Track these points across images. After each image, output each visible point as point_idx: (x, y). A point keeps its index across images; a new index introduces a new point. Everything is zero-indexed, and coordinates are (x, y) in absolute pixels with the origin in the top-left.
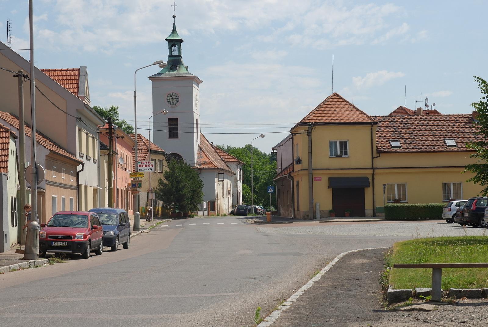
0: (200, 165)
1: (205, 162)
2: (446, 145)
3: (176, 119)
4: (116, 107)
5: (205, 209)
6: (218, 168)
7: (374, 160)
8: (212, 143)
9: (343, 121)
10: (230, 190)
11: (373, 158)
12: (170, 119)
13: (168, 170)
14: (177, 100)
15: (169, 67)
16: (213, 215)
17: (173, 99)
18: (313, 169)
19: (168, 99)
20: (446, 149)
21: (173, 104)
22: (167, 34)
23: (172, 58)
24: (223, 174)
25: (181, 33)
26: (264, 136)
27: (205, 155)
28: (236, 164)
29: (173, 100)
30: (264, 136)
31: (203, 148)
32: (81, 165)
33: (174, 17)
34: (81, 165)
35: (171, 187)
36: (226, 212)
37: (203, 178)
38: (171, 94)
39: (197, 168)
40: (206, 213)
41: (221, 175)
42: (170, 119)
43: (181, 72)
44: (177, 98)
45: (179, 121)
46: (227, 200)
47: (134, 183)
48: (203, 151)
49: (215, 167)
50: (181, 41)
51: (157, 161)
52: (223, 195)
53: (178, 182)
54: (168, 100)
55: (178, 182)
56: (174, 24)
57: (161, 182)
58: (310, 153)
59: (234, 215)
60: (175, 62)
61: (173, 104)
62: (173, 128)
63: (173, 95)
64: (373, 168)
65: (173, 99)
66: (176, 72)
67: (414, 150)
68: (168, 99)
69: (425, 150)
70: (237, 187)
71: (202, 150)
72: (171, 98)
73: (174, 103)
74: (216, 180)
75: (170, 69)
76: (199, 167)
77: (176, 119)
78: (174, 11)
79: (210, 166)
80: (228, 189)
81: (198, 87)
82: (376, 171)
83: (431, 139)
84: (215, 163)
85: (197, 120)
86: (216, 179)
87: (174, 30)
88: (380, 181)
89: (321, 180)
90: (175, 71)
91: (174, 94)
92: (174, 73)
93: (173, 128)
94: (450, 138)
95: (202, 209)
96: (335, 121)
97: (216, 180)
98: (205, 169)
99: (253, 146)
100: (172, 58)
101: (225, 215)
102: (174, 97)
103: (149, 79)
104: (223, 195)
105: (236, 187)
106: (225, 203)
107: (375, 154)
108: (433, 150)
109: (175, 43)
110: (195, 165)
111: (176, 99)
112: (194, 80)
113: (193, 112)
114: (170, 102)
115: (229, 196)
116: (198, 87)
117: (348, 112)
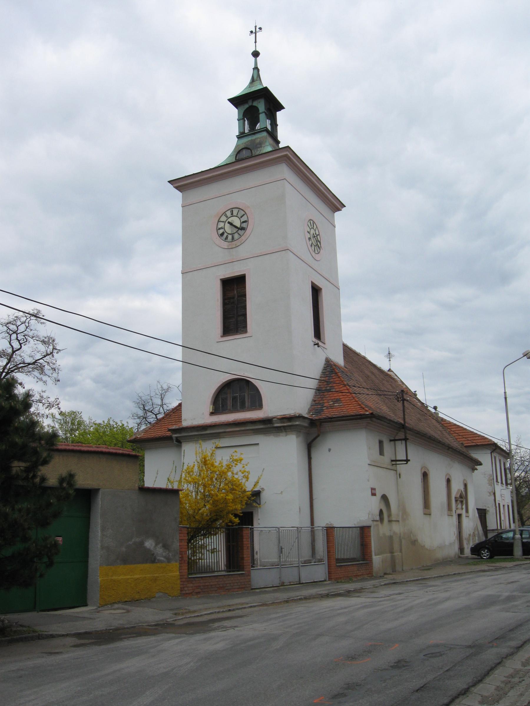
8: (435, 408)
19: (220, 229)
33: (256, 54)
38: (229, 214)
52: (427, 504)
54: (221, 231)
56: (256, 69)
63: (232, 214)
68: (220, 229)
70: (494, 494)
78: (255, 42)
91: (235, 212)
98: (331, 420)
100: (245, 140)
103: (170, 186)
104: (427, 504)
105: (492, 494)
109: (257, 106)
114: (225, 234)
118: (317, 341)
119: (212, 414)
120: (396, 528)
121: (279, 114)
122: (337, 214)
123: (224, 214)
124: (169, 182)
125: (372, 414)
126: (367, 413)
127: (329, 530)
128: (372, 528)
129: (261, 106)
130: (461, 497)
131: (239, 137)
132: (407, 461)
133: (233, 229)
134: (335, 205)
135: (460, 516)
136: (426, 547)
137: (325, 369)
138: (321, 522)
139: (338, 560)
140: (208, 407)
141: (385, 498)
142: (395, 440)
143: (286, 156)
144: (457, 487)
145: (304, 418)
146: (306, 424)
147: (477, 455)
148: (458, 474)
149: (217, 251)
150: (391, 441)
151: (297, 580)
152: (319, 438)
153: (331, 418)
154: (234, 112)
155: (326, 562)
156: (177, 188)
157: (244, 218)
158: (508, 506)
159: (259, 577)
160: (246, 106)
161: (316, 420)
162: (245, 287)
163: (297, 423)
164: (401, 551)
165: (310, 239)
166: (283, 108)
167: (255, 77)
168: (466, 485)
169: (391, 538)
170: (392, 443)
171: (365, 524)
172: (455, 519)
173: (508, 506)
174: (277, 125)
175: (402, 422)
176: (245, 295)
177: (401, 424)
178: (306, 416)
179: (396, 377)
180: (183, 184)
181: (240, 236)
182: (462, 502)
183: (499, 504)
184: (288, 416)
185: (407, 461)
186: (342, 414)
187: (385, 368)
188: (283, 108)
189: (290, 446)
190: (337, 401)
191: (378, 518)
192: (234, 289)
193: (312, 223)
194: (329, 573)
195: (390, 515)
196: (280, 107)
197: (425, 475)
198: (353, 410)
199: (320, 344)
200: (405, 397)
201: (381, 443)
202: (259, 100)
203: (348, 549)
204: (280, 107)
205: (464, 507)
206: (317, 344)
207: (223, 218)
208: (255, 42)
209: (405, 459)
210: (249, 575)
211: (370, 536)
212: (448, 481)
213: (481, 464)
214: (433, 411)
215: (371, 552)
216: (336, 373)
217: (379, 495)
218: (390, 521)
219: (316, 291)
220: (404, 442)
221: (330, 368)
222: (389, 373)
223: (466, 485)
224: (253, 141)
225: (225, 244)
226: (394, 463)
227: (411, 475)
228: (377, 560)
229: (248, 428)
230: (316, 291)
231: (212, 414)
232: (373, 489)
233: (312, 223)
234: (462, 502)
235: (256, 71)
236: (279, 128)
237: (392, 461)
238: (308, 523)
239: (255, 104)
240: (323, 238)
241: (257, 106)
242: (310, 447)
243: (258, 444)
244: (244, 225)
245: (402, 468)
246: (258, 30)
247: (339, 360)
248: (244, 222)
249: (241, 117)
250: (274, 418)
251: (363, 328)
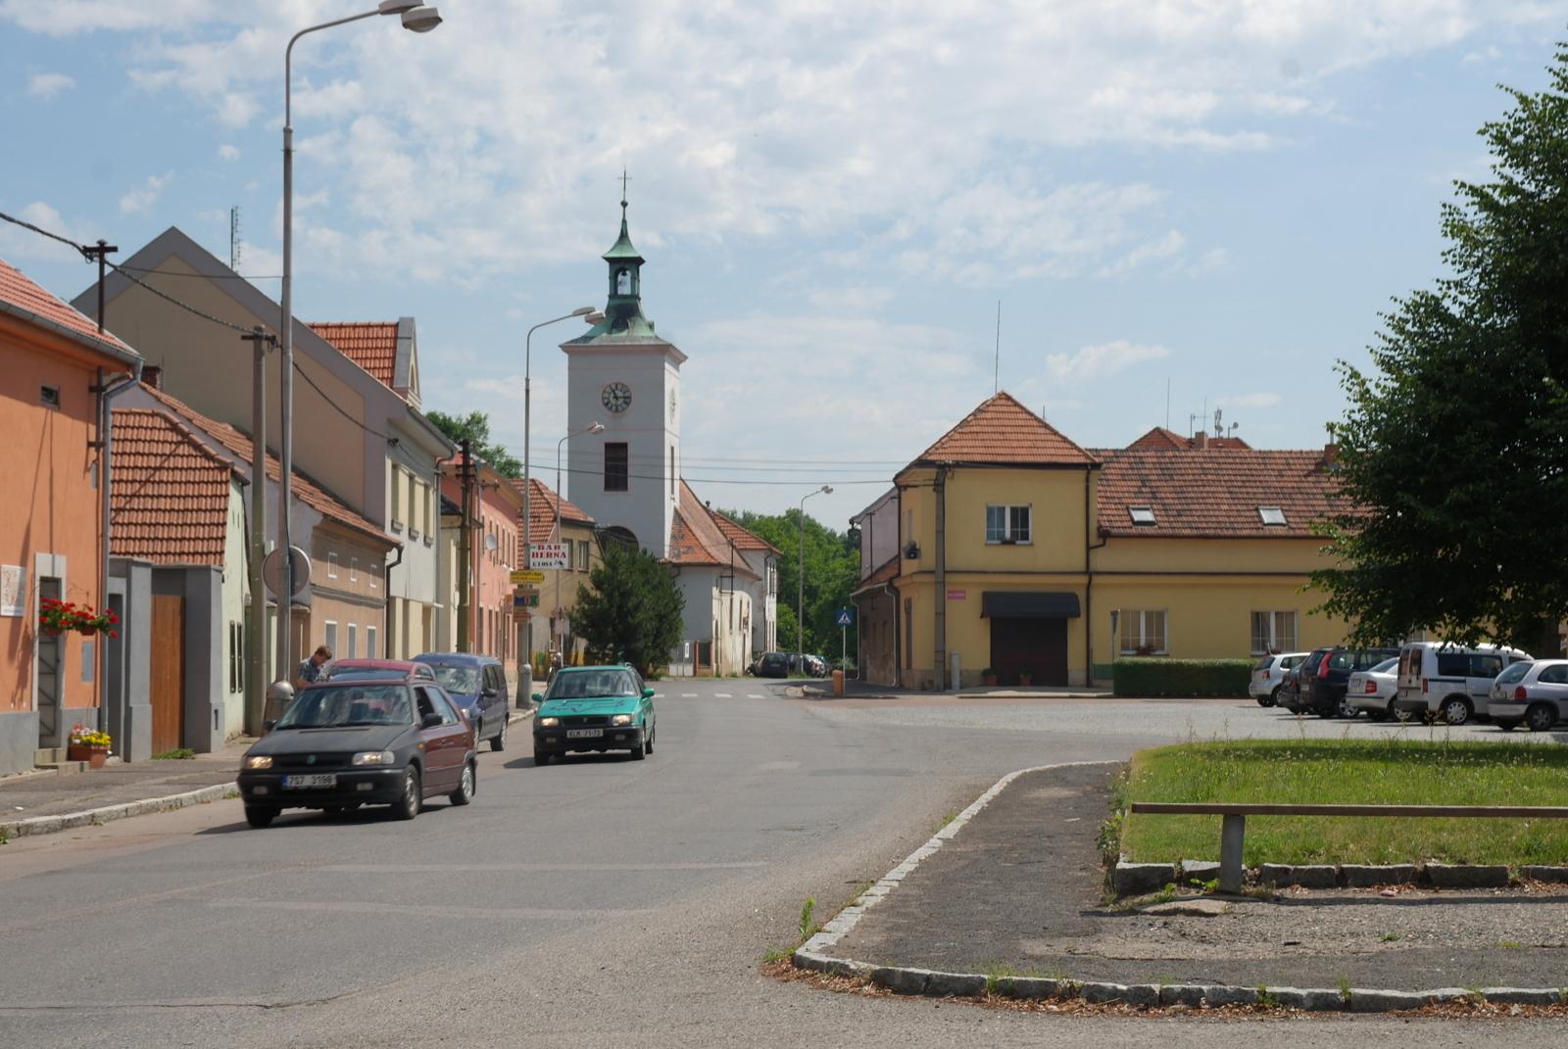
0: (678, 556)
1: (689, 548)
2: (1261, 521)
3: (624, 446)
4: (483, 416)
5: (688, 661)
6: (719, 565)
7: (1093, 553)
8: (708, 503)
9: (1019, 459)
10: (748, 617)
11: (1089, 548)
12: (609, 447)
13: (601, 566)
14: (627, 400)
15: (610, 323)
16: (705, 675)
17: (616, 397)
18: (945, 572)
20: (1261, 533)
21: (617, 408)
22: (607, 247)
23: (617, 302)
24: (732, 577)
25: (641, 242)
26: (832, 490)
27: (690, 531)
28: (763, 555)
29: (618, 400)
30: (832, 490)
31: (685, 514)
32: (395, 551)
33: (624, 204)
34: (395, 551)
35: (607, 606)
36: (738, 669)
38: (614, 387)
39: (670, 562)
40: (689, 670)
41: (727, 582)
42: (609, 447)
43: (638, 334)
44: (627, 395)
45: (631, 451)
46: (739, 639)
47: (520, 596)
48: (685, 522)
49: (713, 561)
50: (639, 261)
51: (575, 545)
52: (731, 627)
53: (626, 595)
54: (606, 401)
55: (626, 595)
56: (624, 222)
57: (584, 595)
58: (940, 532)
59: (757, 675)
60: (623, 311)
61: (617, 408)
62: (616, 466)
64: (1088, 572)
65: (616, 397)
66: (624, 334)
67: (1187, 532)
69: (1212, 532)
70: (765, 609)
71: (682, 519)
72: (612, 395)
73: (620, 409)
74: (715, 591)
75: (612, 327)
76: (674, 560)
77: (624, 446)
79: (702, 558)
80: (744, 615)
81: (678, 370)
82: (1096, 580)
83: (1226, 507)
84: (713, 551)
85: (672, 449)
86: (714, 589)
87: (624, 236)
88: (1103, 604)
89: (964, 598)
90: (622, 331)
91: (619, 387)
92: (622, 337)
93: (616, 466)
94: (1271, 506)
95: (681, 660)
96: (1000, 459)
97: (715, 591)
99: (805, 514)
101: (734, 675)
102: (619, 394)
104: (731, 627)
106: (734, 648)
107: (1094, 540)
108: (1231, 532)
109: (624, 266)
110: (667, 555)
111: (624, 397)
112: (665, 352)
113: (664, 429)
115: (745, 631)
116: (678, 370)
117: (1031, 437)
131: (610, 297)
172: (742, 636)
181: (624, 409)
186: (697, 561)
225: (610, 413)
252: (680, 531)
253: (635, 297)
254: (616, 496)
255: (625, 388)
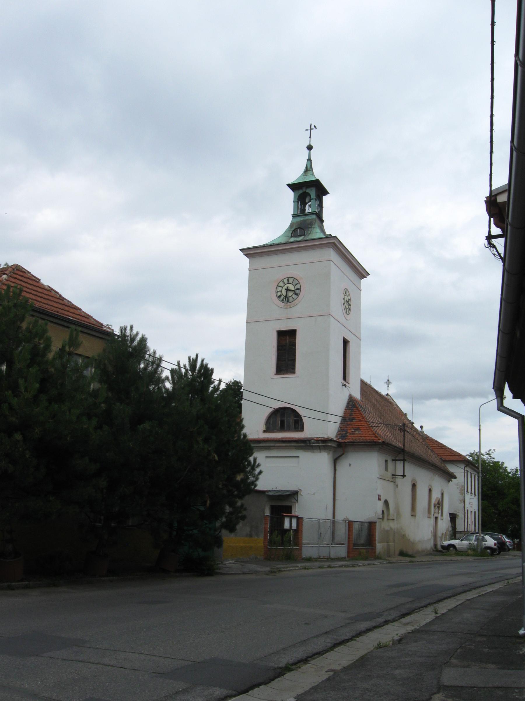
3: (292, 333)
15: (290, 235)
33: (310, 148)
37: (350, 465)
54: (279, 294)
56: (309, 160)
63: (288, 282)
70: (464, 502)
77: (292, 333)
78: (310, 137)
87: (308, 169)
99: (505, 466)
100: (298, 219)
103: (241, 253)
109: (309, 192)
114: (282, 297)
118: (344, 383)
119: (264, 431)
120: (393, 525)
121: (325, 198)
122: (363, 280)
123: (283, 281)
124: (240, 250)
125: (383, 442)
126: (380, 441)
127: (350, 524)
128: (377, 524)
129: (313, 193)
130: (438, 503)
131: (294, 216)
132: (404, 476)
133: (289, 293)
134: (361, 273)
135: (436, 518)
136: (411, 540)
137: (348, 403)
138: (340, 517)
139: (354, 545)
140: (263, 427)
141: (386, 502)
142: (395, 460)
143: (334, 243)
144: (436, 495)
145: (334, 441)
146: (335, 446)
147: (452, 469)
148: (438, 484)
149: (276, 307)
150: (393, 460)
151: (328, 555)
152: (343, 456)
153: (353, 442)
154: (290, 195)
155: (346, 545)
156: (245, 255)
157: (298, 286)
158: (475, 512)
159: (307, 552)
160: (301, 192)
161: (342, 443)
162: (295, 338)
163: (329, 444)
164: (394, 542)
165: (344, 304)
166: (328, 193)
167: (309, 167)
168: (442, 494)
169: (387, 532)
170: (394, 462)
171: (372, 520)
172: (433, 520)
173: (475, 512)
174: (323, 207)
175: (403, 447)
176: (295, 345)
177: (400, 449)
178: (335, 439)
179: (392, 401)
180: (250, 253)
181: (294, 300)
182: (439, 507)
183: (468, 510)
184: (322, 439)
185: (404, 476)
187: (384, 393)
188: (328, 193)
189: (322, 460)
190: (358, 429)
191: (381, 517)
192: (287, 341)
193: (346, 291)
194: (348, 552)
195: (388, 515)
196: (326, 193)
197: (414, 485)
198: (369, 438)
199: (347, 384)
200: (406, 428)
201: (386, 461)
202: (312, 188)
203: (360, 538)
204: (326, 193)
205: (440, 511)
206: (345, 385)
207: (281, 284)
208: (310, 137)
209: (402, 474)
210: (301, 550)
211: (375, 529)
212: (430, 490)
213: (455, 477)
214: (419, 429)
215: (375, 540)
216: (357, 408)
217: (383, 500)
218: (388, 519)
219: (346, 342)
220: (402, 462)
221: (352, 403)
222: (387, 397)
223: (442, 494)
224: (304, 221)
225: (282, 305)
226: (394, 477)
227: (405, 485)
228: (379, 546)
229: (292, 445)
230: (346, 342)
231: (264, 431)
232: (379, 496)
233: (346, 291)
234: (439, 507)
235: (309, 162)
236: (324, 209)
237: (393, 475)
238: (330, 517)
239: (308, 191)
240: (352, 302)
241: (309, 192)
242: (335, 462)
243: (299, 457)
244: (297, 291)
245: (399, 481)
246: (313, 127)
247: (357, 395)
248: (297, 289)
249: (296, 200)
250: (312, 439)
251: (375, 368)
252: (351, 415)
253: (319, 216)
254: (286, 380)
255: (295, 281)
